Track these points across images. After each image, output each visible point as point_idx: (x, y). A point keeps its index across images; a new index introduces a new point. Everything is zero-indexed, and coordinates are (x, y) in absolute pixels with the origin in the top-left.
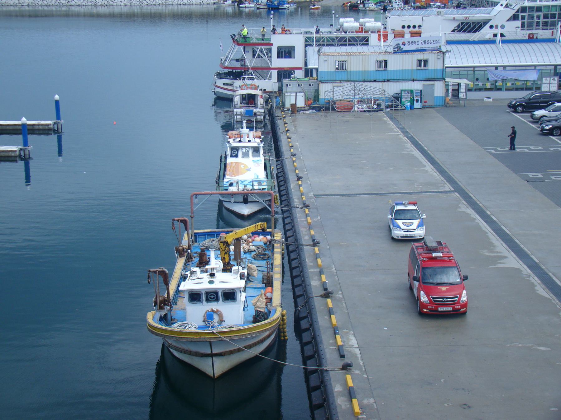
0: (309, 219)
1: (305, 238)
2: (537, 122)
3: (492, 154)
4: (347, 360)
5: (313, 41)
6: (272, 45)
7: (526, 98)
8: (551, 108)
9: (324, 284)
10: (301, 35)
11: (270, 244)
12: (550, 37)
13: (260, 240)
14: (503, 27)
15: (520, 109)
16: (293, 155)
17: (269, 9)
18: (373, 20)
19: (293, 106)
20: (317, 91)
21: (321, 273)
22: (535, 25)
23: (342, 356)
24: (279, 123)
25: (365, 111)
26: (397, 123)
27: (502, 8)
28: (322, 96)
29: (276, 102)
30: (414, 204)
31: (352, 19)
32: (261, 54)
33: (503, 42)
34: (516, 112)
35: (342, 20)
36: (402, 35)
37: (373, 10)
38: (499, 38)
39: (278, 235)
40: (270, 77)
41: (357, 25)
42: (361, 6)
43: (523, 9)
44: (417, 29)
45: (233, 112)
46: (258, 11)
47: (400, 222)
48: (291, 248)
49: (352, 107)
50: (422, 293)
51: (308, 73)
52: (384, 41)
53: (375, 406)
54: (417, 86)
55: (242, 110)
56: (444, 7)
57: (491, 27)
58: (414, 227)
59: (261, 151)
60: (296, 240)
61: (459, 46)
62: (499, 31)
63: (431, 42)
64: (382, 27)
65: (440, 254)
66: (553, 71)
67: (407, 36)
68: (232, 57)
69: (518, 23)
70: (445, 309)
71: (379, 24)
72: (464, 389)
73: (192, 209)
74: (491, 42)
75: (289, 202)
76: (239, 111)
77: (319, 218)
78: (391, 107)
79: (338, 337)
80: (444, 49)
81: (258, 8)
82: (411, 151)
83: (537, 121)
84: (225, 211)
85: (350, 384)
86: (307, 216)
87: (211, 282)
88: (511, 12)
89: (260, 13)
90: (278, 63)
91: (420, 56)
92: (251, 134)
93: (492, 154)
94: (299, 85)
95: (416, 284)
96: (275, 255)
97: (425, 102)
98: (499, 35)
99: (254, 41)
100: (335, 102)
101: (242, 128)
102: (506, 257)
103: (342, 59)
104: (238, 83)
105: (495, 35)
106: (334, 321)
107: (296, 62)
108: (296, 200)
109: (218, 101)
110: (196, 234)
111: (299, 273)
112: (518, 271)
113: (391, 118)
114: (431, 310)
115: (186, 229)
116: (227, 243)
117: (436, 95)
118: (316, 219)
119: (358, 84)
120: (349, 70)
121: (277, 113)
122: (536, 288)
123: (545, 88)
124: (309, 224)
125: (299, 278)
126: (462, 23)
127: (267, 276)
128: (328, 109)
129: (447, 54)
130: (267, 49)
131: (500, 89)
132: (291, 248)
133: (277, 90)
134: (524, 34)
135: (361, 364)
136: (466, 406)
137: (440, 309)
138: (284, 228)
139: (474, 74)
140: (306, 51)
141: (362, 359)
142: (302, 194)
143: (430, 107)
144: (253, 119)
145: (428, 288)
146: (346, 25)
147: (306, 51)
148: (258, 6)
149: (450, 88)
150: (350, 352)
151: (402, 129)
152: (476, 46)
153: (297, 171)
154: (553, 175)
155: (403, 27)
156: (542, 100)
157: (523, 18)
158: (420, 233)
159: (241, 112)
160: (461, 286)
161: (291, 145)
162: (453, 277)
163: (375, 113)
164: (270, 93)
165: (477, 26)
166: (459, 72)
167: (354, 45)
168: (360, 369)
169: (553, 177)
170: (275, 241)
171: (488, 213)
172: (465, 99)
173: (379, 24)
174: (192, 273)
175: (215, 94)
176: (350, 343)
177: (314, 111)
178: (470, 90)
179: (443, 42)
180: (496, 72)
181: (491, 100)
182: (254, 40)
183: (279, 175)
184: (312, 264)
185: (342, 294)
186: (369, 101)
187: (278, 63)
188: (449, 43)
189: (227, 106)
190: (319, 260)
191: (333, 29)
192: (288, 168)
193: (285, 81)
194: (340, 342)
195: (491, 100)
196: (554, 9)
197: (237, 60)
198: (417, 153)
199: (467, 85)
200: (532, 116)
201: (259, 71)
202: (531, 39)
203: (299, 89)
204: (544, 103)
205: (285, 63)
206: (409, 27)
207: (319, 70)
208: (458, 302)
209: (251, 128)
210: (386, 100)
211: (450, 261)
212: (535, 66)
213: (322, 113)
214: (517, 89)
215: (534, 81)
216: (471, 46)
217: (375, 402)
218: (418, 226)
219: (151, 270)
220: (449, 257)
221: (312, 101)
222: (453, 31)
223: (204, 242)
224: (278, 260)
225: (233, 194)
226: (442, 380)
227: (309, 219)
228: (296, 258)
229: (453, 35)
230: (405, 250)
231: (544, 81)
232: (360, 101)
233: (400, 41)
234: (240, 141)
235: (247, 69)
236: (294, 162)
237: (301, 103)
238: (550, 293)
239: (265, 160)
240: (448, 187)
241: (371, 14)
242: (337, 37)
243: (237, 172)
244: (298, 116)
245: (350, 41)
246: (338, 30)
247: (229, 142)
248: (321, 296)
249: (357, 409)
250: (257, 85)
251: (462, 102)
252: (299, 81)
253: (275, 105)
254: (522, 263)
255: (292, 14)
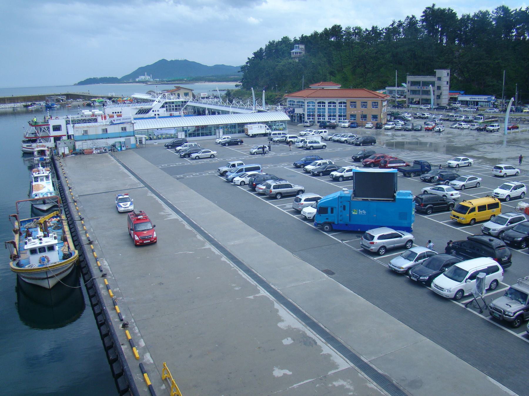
0: (77, 208)
1: (76, 217)
2: (178, 152)
3: (160, 168)
4: (104, 272)
5: (70, 122)
6: (49, 125)
7: (172, 142)
8: (183, 145)
9: (88, 238)
10: (64, 120)
11: (60, 222)
12: (179, 115)
13: (55, 220)
14: (158, 111)
15: (170, 147)
16: (66, 178)
17: (46, 108)
18: (98, 110)
19: (63, 154)
20: (74, 146)
21: (86, 233)
22: (172, 110)
23: (101, 271)
24: (57, 162)
25: (99, 153)
26: (115, 157)
27: (157, 103)
28: (77, 148)
29: (55, 152)
30: (127, 195)
31: (88, 111)
32: (44, 130)
33: (159, 117)
34: (168, 148)
35: (83, 111)
36: (113, 117)
37: (98, 106)
38: (157, 116)
39: (64, 217)
40: (50, 141)
41: (91, 113)
42: (92, 104)
43: (166, 103)
44: (119, 114)
45: (34, 159)
46: (41, 109)
47: (121, 204)
48: (70, 223)
49: (92, 152)
50: (135, 235)
51: (69, 137)
52: (105, 120)
53: (120, 291)
54: (122, 140)
55: (38, 158)
56: (131, 103)
57: (153, 111)
58: (128, 205)
59: (50, 178)
60: (72, 218)
61: (140, 120)
62: (157, 113)
63: (127, 119)
64: (103, 114)
65: (142, 217)
66: (182, 130)
67: (115, 117)
68: (30, 132)
69: (165, 109)
70: (147, 242)
71: (101, 112)
72: (159, 276)
73: (17, 210)
74: (154, 118)
75: (66, 201)
76: (37, 158)
77: (82, 206)
78: (111, 150)
79: (98, 262)
80: (133, 122)
81: (41, 108)
82: (123, 170)
83: (178, 152)
84: (34, 209)
85: (107, 283)
86: (76, 206)
87: (41, 243)
88: (161, 105)
89: (42, 110)
90: (53, 133)
91: (122, 126)
92: (44, 169)
93: (160, 168)
94: (65, 143)
95: (132, 232)
96: (65, 226)
97: (127, 147)
98: (157, 115)
99: (40, 124)
100: (84, 150)
101: (39, 167)
102: (171, 214)
103: (85, 129)
104: (34, 145)
105: (155, 115)
106: (95, 255)
107: (63, 132)
108: (69, 199)
109: (24, 155)
110: (21, 222)
111: (75, 234)
112: (177, 220)
113: (112, 156)
114: (140, 243)
115: (17, 219)
116: (41, 223)
117: (132, 143)
118: (81, 207)
119: (94, 141)
120: (89, 134)
121: (56, 158)
122: (185, 226)
123: (179, 137)
124: (78, 210)
125: (75, 237)
126: (140, 110)
127: (64, 237)
128: (81, 154)
129: (135, 124)
130: (48, 127)
131: (160, 139)
132: (70, 223)
133: (54, 147)
134: (168, 114)
135: (111, 273)
136: (161, 284)
137: (145, 242)
138: (66, 214)
139: (148, 132)
140: (67, 127)
141: (111, 271)
142: (72, 196)
143: (130, 149)
144: (44, 162)
145: (136, 232)
146: (85, 113)
147: (67, 127)
148: (41, 107)
149: (138, 140)
150: (105, 268)
151: (117, 160)
152: (147, 120)
153: (69, 185)
154: (187, 175)
155: (113, 113)
156: (179, 142)
157: (167, 107)
158: (131, 208)
159: (38, 159)
160: (152, 230)
161: (64, 172)
162: (149, 226)
163: (104, 154)
164: (51, 148)
165: (147, 111)
166: (141, 132)
167: (90, 122)
168: (111, 276)
169: (187, 176)
170: (63, 219)
171: (161, 195)
172: (145, 144)
173: (101, 112)
174: (29, 240)
175: (23, 151)
176: (104, 264)
177: (74, 155)
178: (147, 140)
179: (132, 119)
180: (158, 131)
181: (157, 144)
182: (40, 123)
183: (60, 188)
184: (81, 229)
185: (98, 242)
186: (100, 148)
187: (53, 133)
188: (135, 119)
189: (31, 157)
190: (84, 227)
191: (79, 116)
192: (64, 184)
193: (58, 142)
194: (99, 265)
195: (157, 144)
196: (179, 103)
197: (33, 134)
198: (126, 171)
199: (145, 138)
200: (176, 150)
201: (44, 138)
202: (171, 116)
203: (65, 145)
204: (180, 143)
205: (57, 133)
206: (116, 113)
207: (75, 135)
208: (153, 238)
209: (43, 166)
210: (109, 147)
211: (147, 219)
212: (174, 128)
213: (78, 156)
214: (168, 138)
215: (175, 134)
216: (145, 120)
217: (120, 289)
218: (130, 205)
219: (7, 242)
220: (146, 218)
221: (72, 150)
222: (136, 114)
223: (26, 225)
224: (66, 228)
225: (38, 200)
226: (149, 274)
227: (77, 208)
228: (73, 227)
229: (136, 115)
230: (126, 217)
231: (179, 134)
232: (96, 149)
233: (112, 119)
234: (39, 174)
235: (38, 137)
236: (66, 181)
237: (67, 152)
238: (191, 227)
239: (52, 181)
240: (142, 185)
241: (97, 107)
242: (82, 119)
243: (39, 188)
244: (66, 158)
245: (88, 121)
246: (82, 116)
247: (33, 174)
248: (87, 244)
249: (112, 294)
250: (45, 145)
251: (144, 146)
252: (65, 141)
253: (54, 154)
254: (178, 216)
255: (58, 109)
